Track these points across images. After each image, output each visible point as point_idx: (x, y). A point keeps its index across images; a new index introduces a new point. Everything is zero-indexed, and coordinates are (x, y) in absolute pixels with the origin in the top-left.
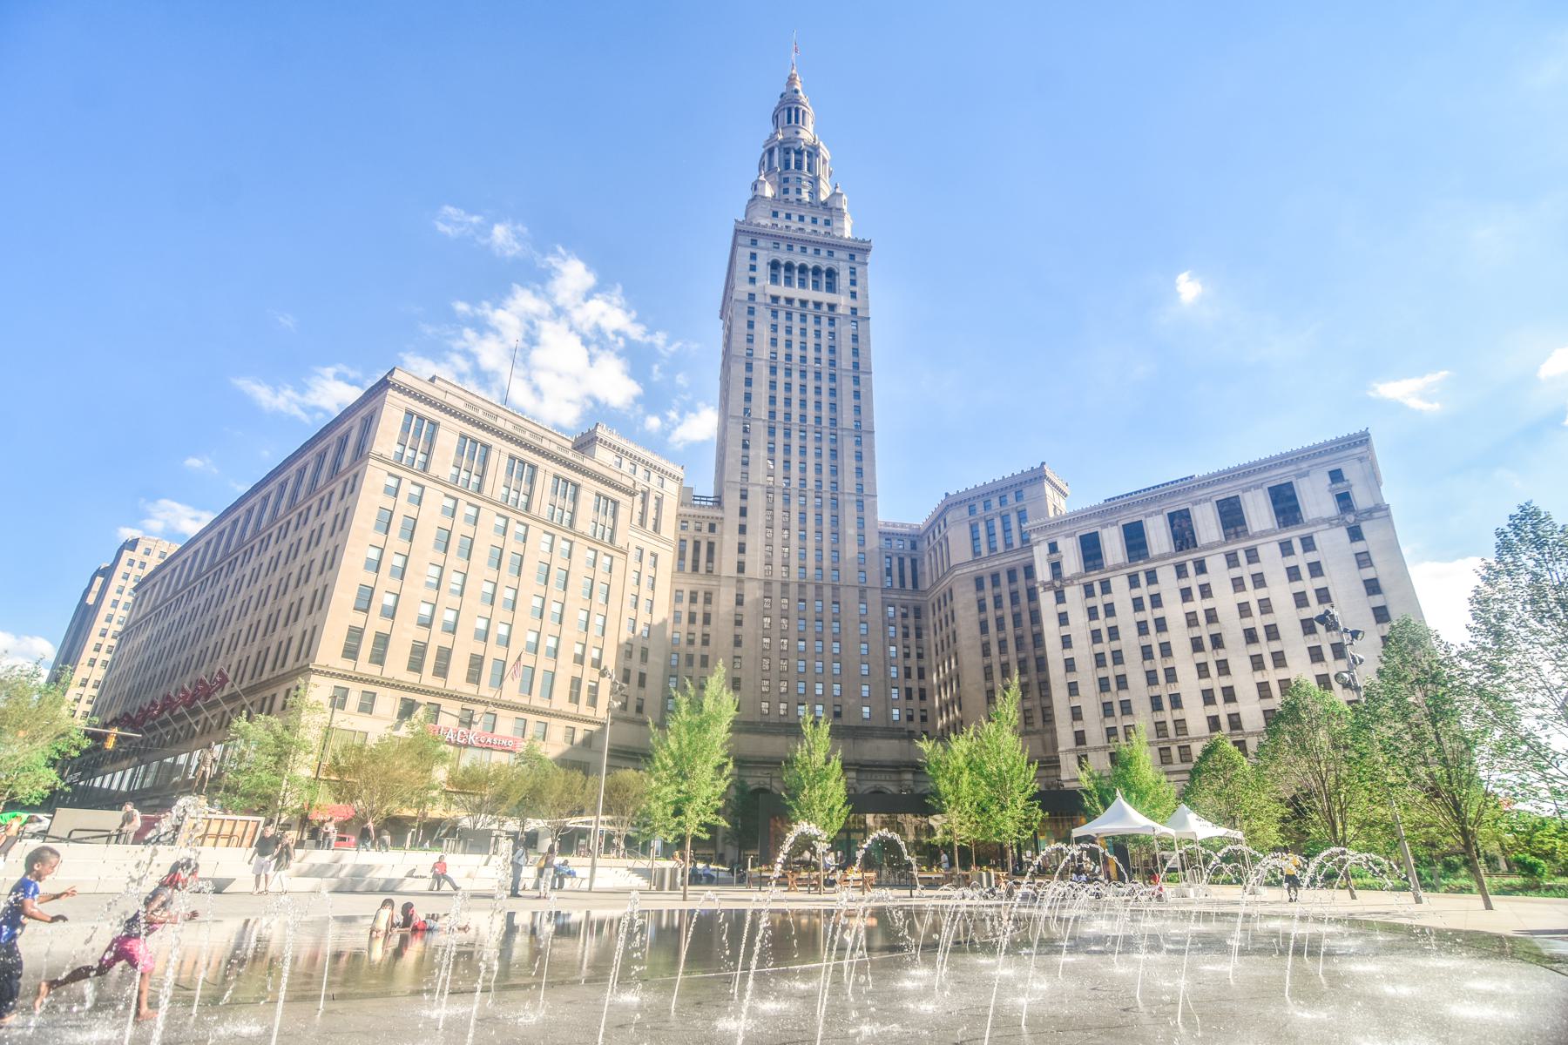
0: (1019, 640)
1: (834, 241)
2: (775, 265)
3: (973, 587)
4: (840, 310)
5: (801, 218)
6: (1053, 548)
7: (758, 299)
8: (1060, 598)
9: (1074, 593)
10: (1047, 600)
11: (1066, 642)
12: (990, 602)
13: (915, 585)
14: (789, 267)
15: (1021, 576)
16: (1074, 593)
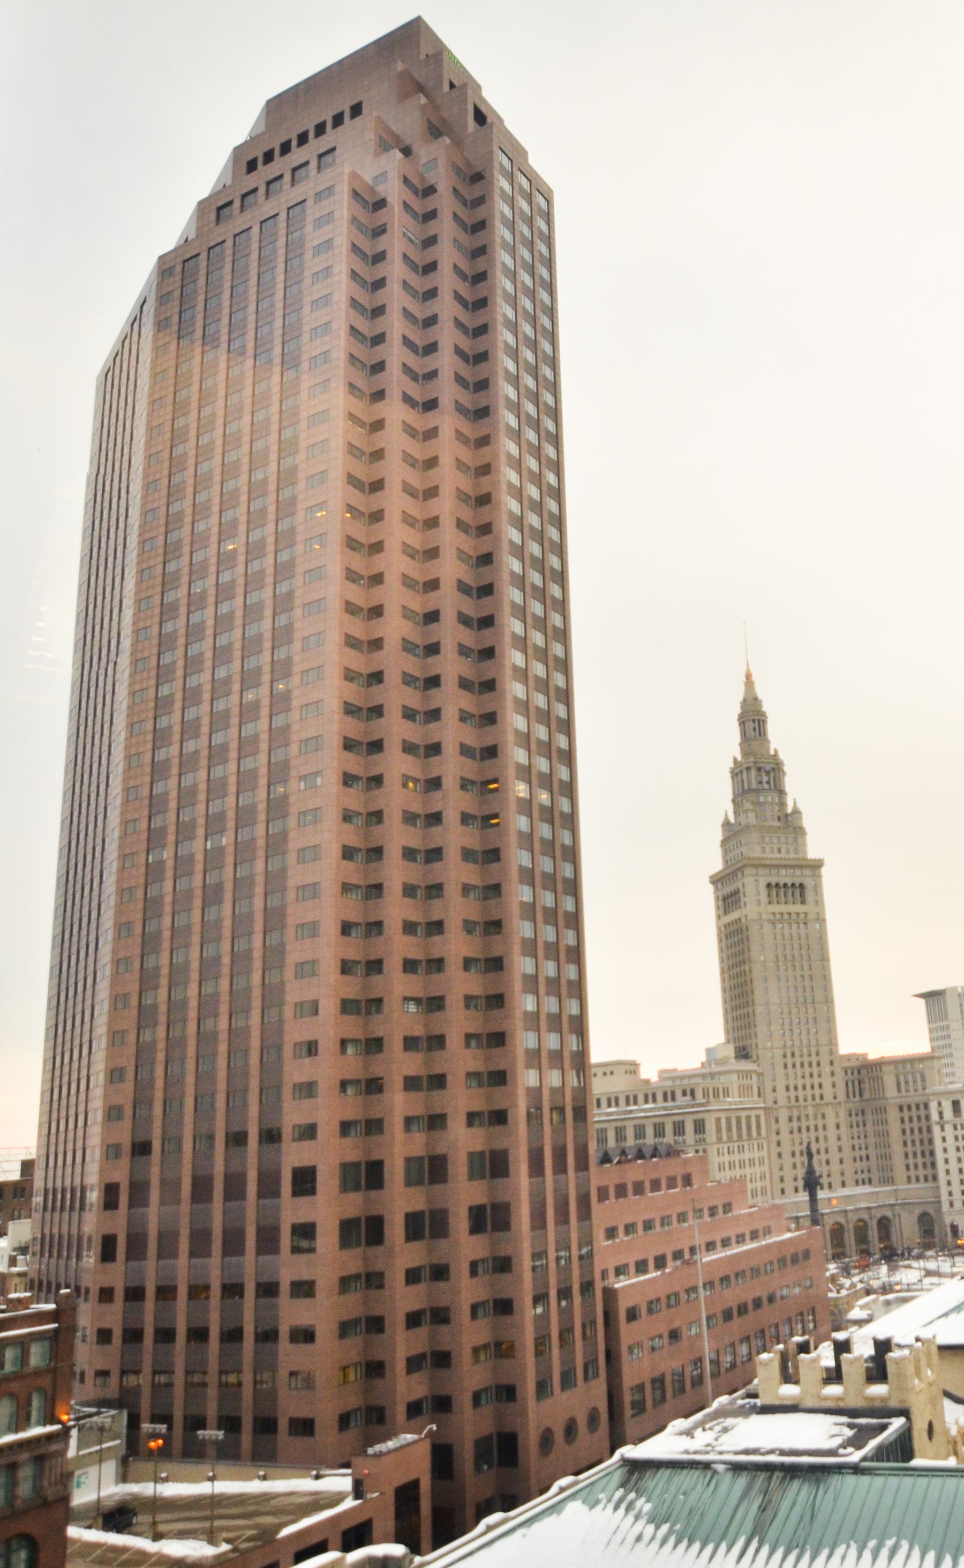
0: (922, 1141)
1: (802, 863)
2: (769, 885)
3: (897, 1110)
4: (809, 916)
5: (779, 838)
6: (940, 1104)
7: (764, 916)
8: (943, 1129)
9: (949, 1128)
10: (936, 1130)
11: (945, 1150)
12: (906, 1119)
13: (861, 1095)
14: (777, 885)
15: (922, 1107)
16: (949, 1128)
